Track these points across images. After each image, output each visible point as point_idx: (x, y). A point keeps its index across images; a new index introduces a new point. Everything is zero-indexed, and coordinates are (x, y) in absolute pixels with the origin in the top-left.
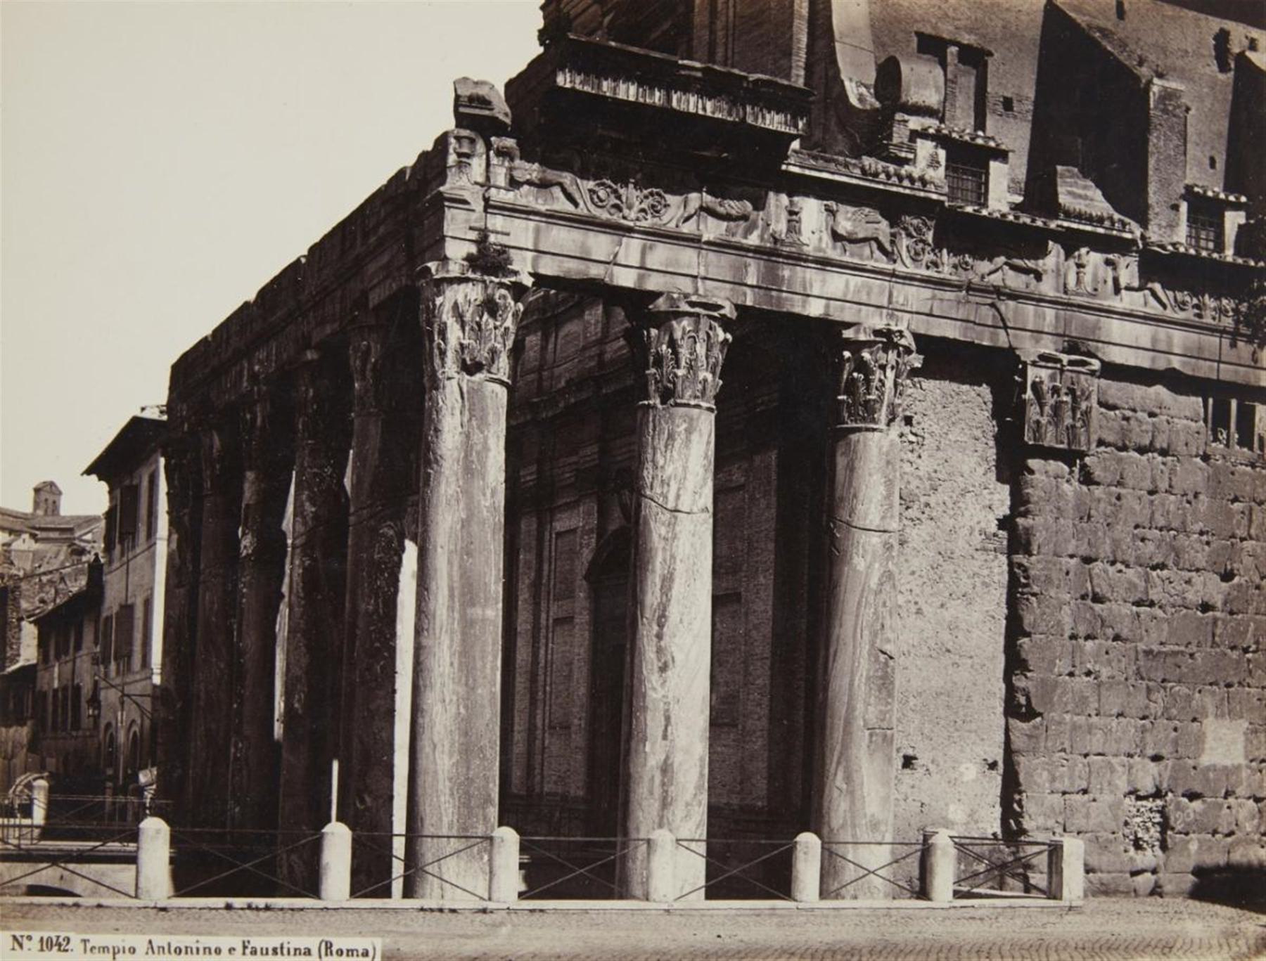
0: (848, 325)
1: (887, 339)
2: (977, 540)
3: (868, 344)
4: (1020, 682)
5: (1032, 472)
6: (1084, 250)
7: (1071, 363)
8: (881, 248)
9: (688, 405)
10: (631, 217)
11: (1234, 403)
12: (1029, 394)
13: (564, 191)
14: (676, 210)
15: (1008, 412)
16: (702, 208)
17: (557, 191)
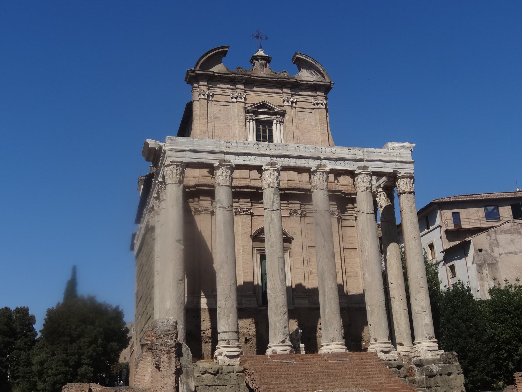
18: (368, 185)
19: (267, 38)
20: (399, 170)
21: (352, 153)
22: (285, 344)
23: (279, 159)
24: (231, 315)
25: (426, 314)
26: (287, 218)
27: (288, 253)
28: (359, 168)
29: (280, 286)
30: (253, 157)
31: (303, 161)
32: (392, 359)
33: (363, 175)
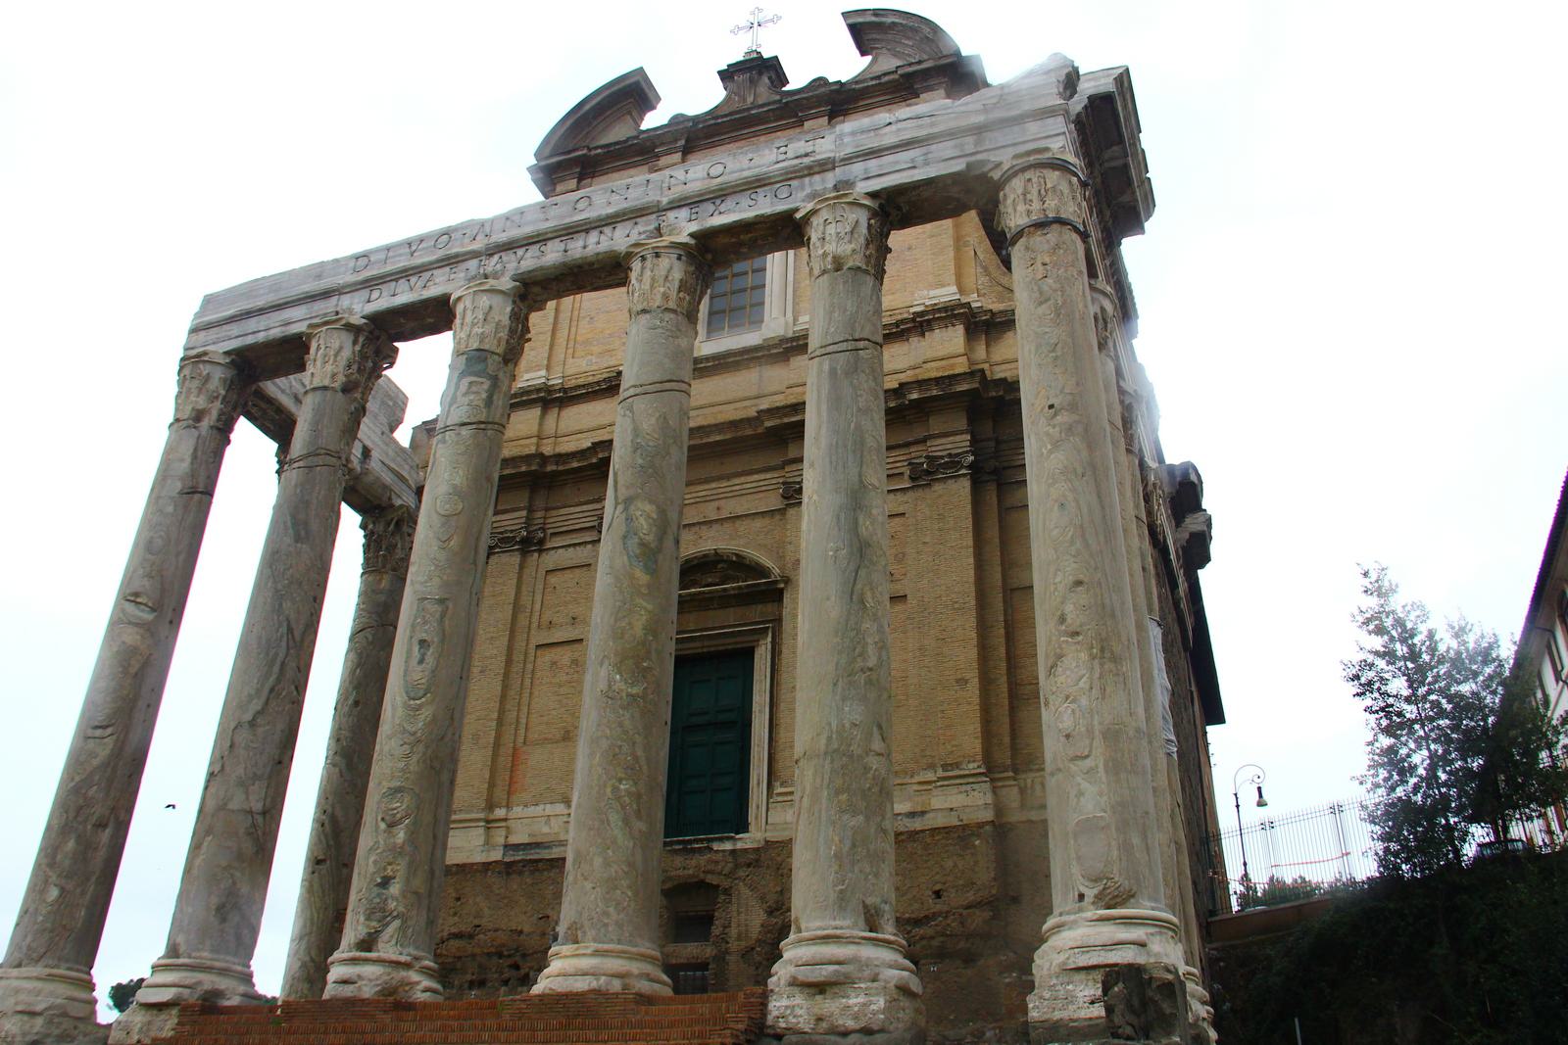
18: (845, 248)
19: (779, 18)
20: (994, 158)
21: (790, 155)
22: (373, 955)
23: (508, 257)
24: (210, 838)
25: (1090, 772)
26: (778, 517)
27: (769, 639)
28: (813, 196)
29: (400, 712)
30: (426, 275)
31: (593, 237)
32: (851, 1024)
33: (824, 214)
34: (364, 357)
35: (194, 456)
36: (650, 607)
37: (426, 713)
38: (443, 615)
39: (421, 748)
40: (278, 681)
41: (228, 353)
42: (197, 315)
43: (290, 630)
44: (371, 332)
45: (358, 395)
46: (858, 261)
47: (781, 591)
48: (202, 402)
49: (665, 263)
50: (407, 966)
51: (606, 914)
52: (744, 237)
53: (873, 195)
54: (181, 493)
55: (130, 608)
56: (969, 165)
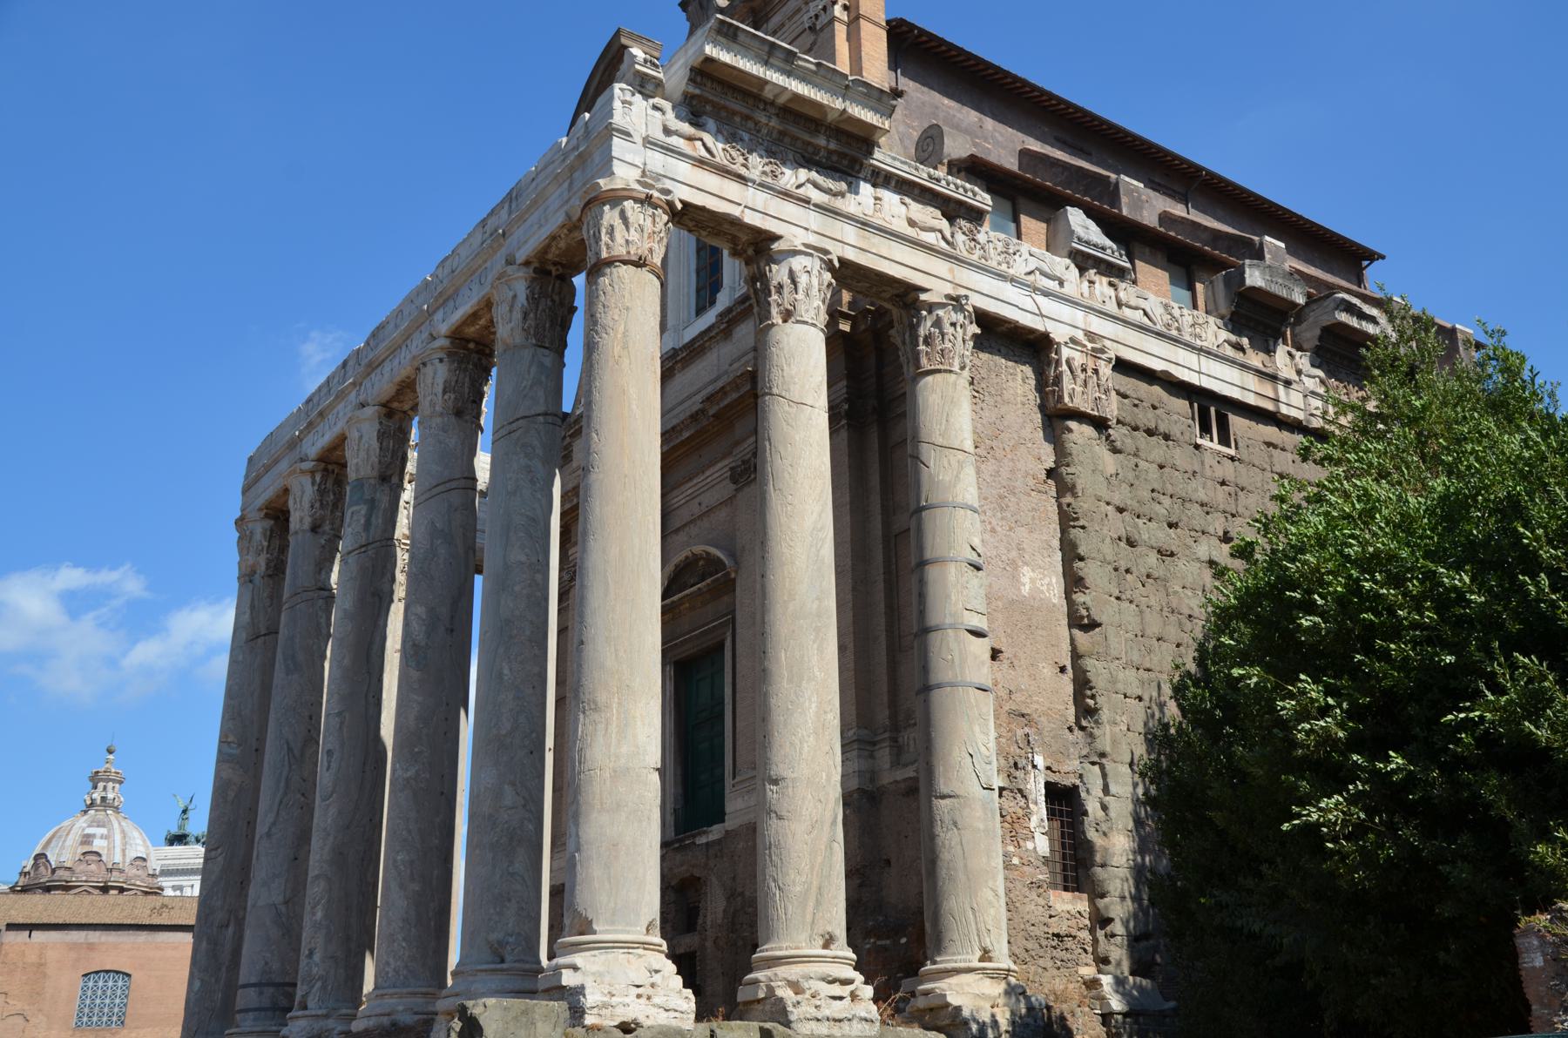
0: (925, 290)
1: (956, 302)
2: (1031, 482)
3: (942, 306)
4: (1079, 598)
5: (1070, 431)
6: (1092, 272)
7: (1093, 349)
8: (944, 238)
9: (805, 323)
10: (754, 174)
11: (1213, 410)
12: (1065, 367)
13: (704, 145)
14: (791, 177)
15: (1047, 385)
16: (808, 181)
17: (699, 143)
34: (322, 492)
35: (252, 607)
36: (420, 699)
37: (333, 811)
38: (342, 723)
39: (331, 838)
40: (285, 794)
41: (260, 509)
42: (246, 477)
43: (290, 749)
44: (325, 470)
45: (327, 527)
46: (519, 338)
47: (734, 580)
48: (251, 559)
49: (429, 370)
50: (327, 1016)
51: (388, 963)
52: (482, 322)
53: (527, 263)
54: (247, 641)
55: (226, 749)
56: (567, 214)
